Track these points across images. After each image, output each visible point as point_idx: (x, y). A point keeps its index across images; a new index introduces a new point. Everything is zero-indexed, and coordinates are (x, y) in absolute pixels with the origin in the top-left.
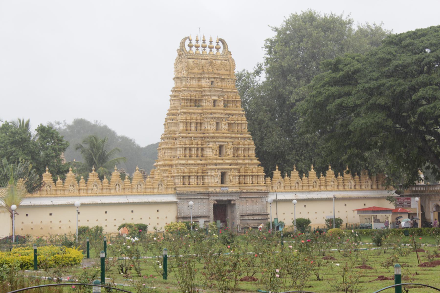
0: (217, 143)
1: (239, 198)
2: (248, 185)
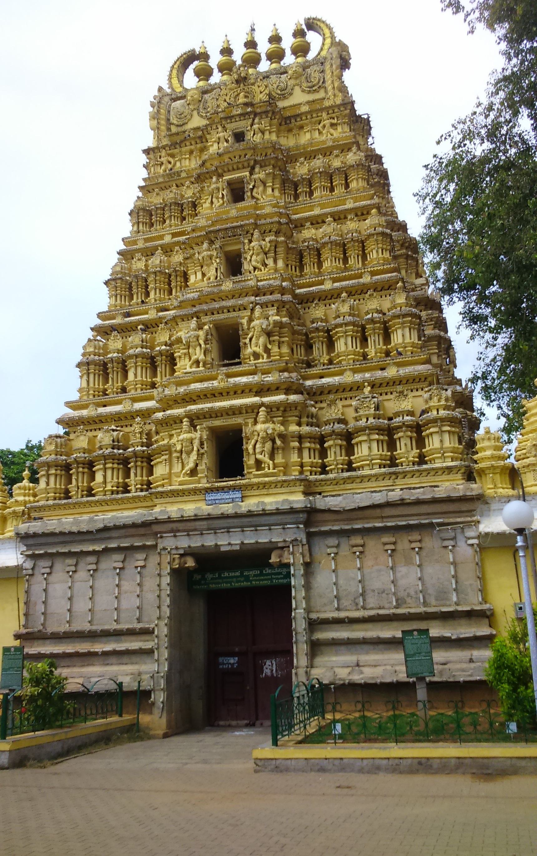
0: (205, 319)
1: (302, 537)
2: (367, 472)
